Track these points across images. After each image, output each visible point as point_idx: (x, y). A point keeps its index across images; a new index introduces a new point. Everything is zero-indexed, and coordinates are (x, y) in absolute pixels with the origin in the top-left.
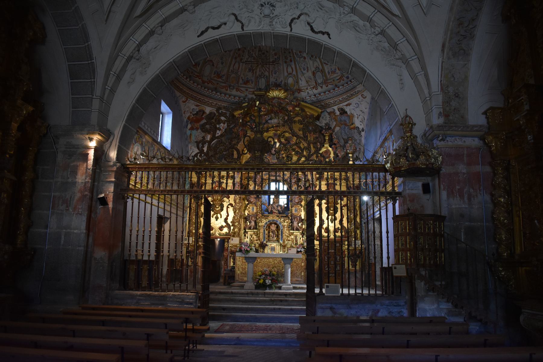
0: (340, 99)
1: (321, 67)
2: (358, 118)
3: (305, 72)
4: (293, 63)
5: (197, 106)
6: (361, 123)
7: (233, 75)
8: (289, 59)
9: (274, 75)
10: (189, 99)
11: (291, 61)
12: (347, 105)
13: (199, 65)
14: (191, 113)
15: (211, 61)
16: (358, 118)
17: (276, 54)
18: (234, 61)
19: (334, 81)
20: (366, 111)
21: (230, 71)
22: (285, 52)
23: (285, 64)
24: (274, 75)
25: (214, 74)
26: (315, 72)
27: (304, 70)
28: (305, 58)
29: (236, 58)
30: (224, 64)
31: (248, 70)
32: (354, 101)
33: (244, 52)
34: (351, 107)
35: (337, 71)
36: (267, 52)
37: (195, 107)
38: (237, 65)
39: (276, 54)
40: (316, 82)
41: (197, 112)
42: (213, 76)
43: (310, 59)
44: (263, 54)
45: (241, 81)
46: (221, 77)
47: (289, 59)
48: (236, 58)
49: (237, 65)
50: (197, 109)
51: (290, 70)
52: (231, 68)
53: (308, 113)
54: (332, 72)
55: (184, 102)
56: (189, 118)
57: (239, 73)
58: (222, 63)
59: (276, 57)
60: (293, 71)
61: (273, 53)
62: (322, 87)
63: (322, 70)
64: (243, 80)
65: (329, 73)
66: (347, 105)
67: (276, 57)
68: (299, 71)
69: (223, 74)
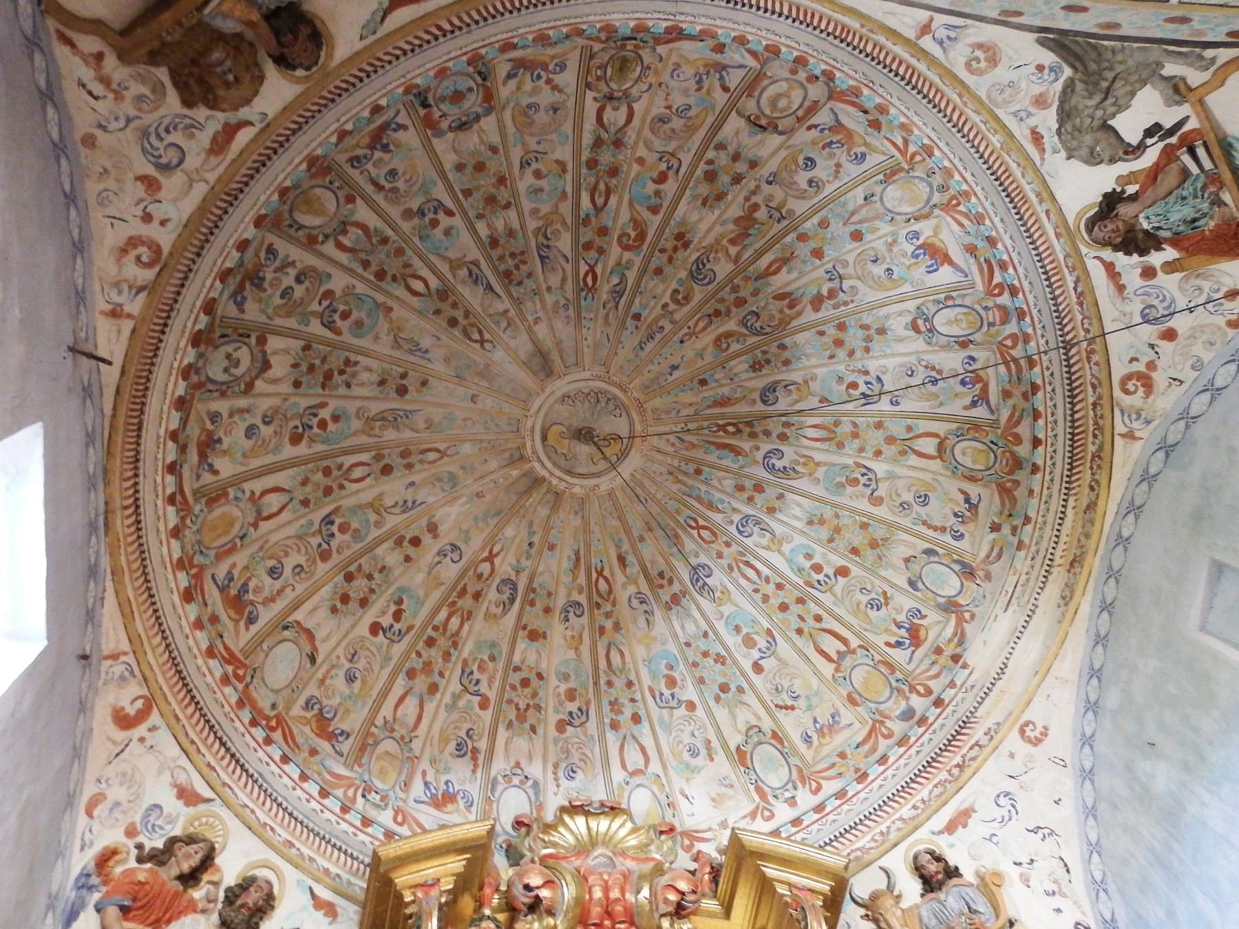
0: (906, 812)
1: (767, 724)
2: (1026, 881)
3: (701, 761)
4: (645, 728)
5: (187, 796)
6: (1057, 902)
7: (388, 745)
8: (628, 712)
9: (563, 781)
10: (155, 718)
11: (636, 719)
12: (950, 828)
13: (251, 621)
14: (131, 832)
15: (310, 635)
16: (1026, 881)
17: (571, 695)
18: (401, 683)
19: (842, 755)
20: (1065, 818)
21: (379, 721)
22: (610, 684)
23: (611, 736)
24: (564, 782)
25: (308, 706)
26: (748, 748)
27: (694, 753)
28: (691, 706)
29: (411, 674)
30: (357, 685)
31: (452, 746)
32: (979, 790)
33: (447, 656)
34: (977, 828)
35: (847, 716)
36: (540, 676)
37: (172, 804)
38: (411, 705)
39: (571, 695)
40: (759, 790)
41: (172, 841)
42: (297, 710)
43: (717, 699)
44: (525, 683)
45: (417, 789)
46: (331, 737)
47: (628, 712)
48: (411, 674)
49: (411, 705)
50: (179, 819)
51: (634, 758)
52: (386, 711)
53: (781, 889)
54: (821, 733)
55: (124, 721)
56: (105, 859)
57: (416, 745)
58: (351, 679)
59: (573, 707)
60: (647, 760)
61: (563, 687)
62: (792, 802)
63: (775, 735)
64: (426, 784)
65: (807, 739)
66: (950, 828)
67: (573, 707)
68: (671, 762)
69: (345, 726)
